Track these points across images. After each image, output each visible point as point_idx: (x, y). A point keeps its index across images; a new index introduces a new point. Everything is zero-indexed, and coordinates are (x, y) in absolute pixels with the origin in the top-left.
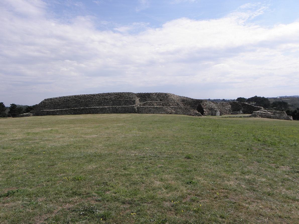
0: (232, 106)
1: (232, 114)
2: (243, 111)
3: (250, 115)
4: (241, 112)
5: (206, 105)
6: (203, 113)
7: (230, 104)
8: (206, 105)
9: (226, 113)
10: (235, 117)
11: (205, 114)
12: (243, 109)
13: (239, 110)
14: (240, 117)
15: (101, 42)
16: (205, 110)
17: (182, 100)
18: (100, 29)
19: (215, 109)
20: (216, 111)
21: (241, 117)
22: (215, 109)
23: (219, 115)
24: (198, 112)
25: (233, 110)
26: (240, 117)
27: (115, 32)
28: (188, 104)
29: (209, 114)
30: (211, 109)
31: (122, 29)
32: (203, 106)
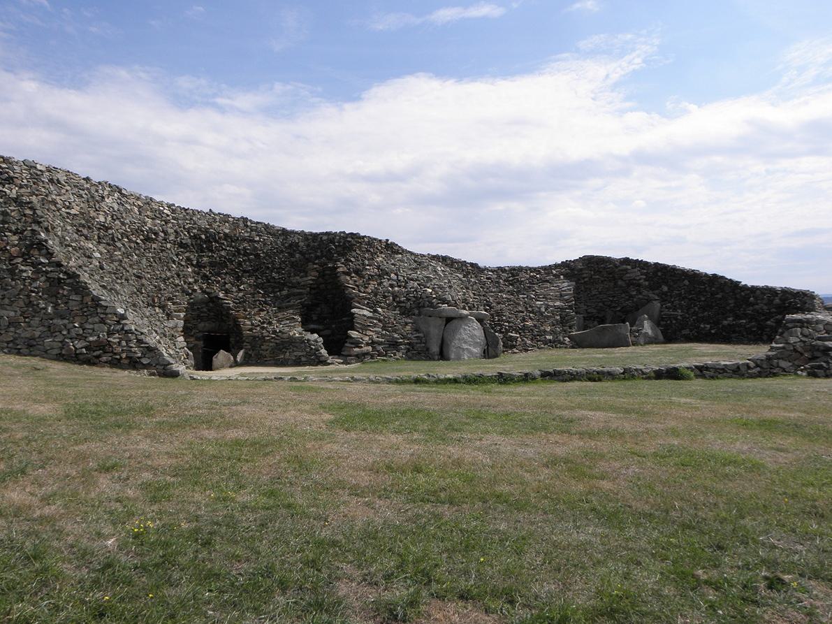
0: (577, 289)
1: (578, 344)
2: (658, 324)
3: (760, 351)
4: (648, 328)
5: (383, 273)
6: (338, 346)
7: (567, 276)
8: (383, 273)
9: (539, 340)
10: (611, 376)
11: (357, 344)
12: (657, 305)
13: (628, 314)
14: (659, 375)
15: (189, 141)
16: (361, 312)
17: (195, 237)
18: (183, 102)
19: (444, 301)
20: (449, 320)
21: (673, 374)
22: (444, 301)
23: (477, 351)
24: (297, 331)
25: (591, 319)
26: (659, 375)
27: (221, 110)
28: (240, 264)
29: (394, 345)
30: (416, 306)
31: (245, 100)
32: (350, 282)
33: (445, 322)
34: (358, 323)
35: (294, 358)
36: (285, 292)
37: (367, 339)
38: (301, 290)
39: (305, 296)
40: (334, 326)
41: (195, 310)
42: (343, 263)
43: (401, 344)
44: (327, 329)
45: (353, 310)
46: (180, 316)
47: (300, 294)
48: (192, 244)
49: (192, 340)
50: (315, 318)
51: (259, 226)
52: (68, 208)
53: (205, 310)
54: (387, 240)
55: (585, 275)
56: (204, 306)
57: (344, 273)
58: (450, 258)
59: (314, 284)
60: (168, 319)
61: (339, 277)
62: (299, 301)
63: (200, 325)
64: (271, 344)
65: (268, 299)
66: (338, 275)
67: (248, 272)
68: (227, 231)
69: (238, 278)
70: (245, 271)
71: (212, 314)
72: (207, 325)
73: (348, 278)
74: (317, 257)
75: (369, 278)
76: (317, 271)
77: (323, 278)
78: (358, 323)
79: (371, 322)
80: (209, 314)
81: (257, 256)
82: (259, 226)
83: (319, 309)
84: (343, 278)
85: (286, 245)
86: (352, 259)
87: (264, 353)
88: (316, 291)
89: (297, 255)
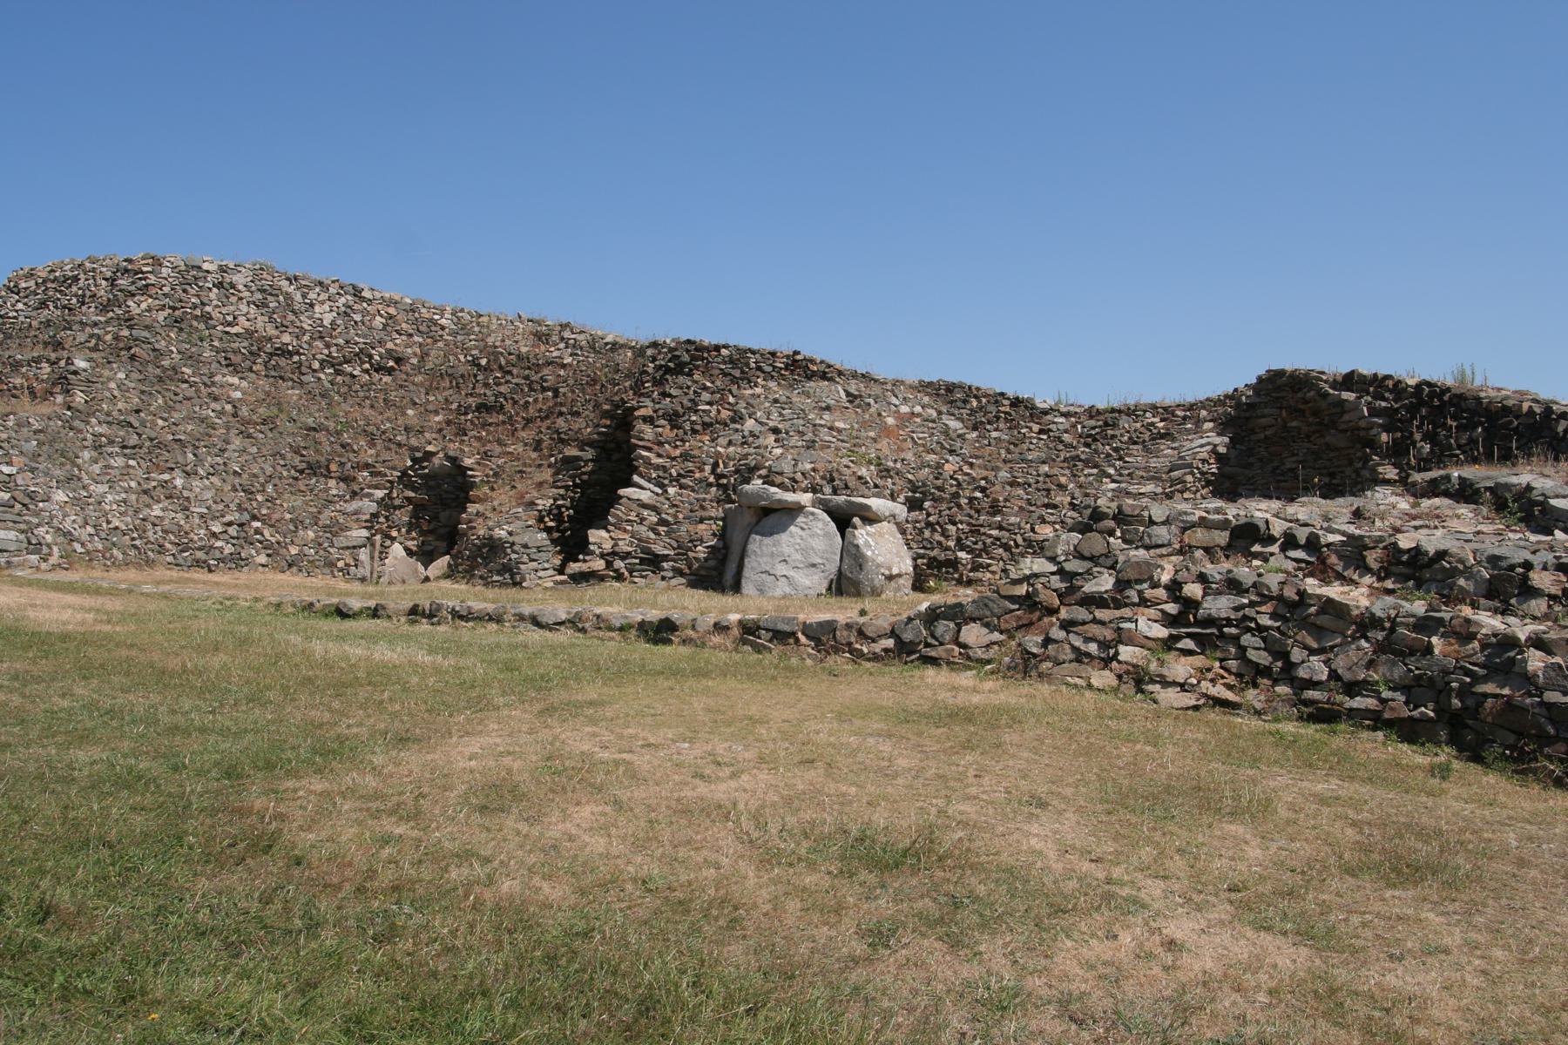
16: (640, 492)
20: (767, 511)
33: (754, 520)
43: (666, 558)
45: (622, 492)
51: (581, 337)
52: (230, 324)
54: (796, 353)
55: (1263, 421)
57: (646, 419)
58: (961, 386)
68: (524, 350)
75: (694, 431)
82: (581, 337)
86: (674, 392)
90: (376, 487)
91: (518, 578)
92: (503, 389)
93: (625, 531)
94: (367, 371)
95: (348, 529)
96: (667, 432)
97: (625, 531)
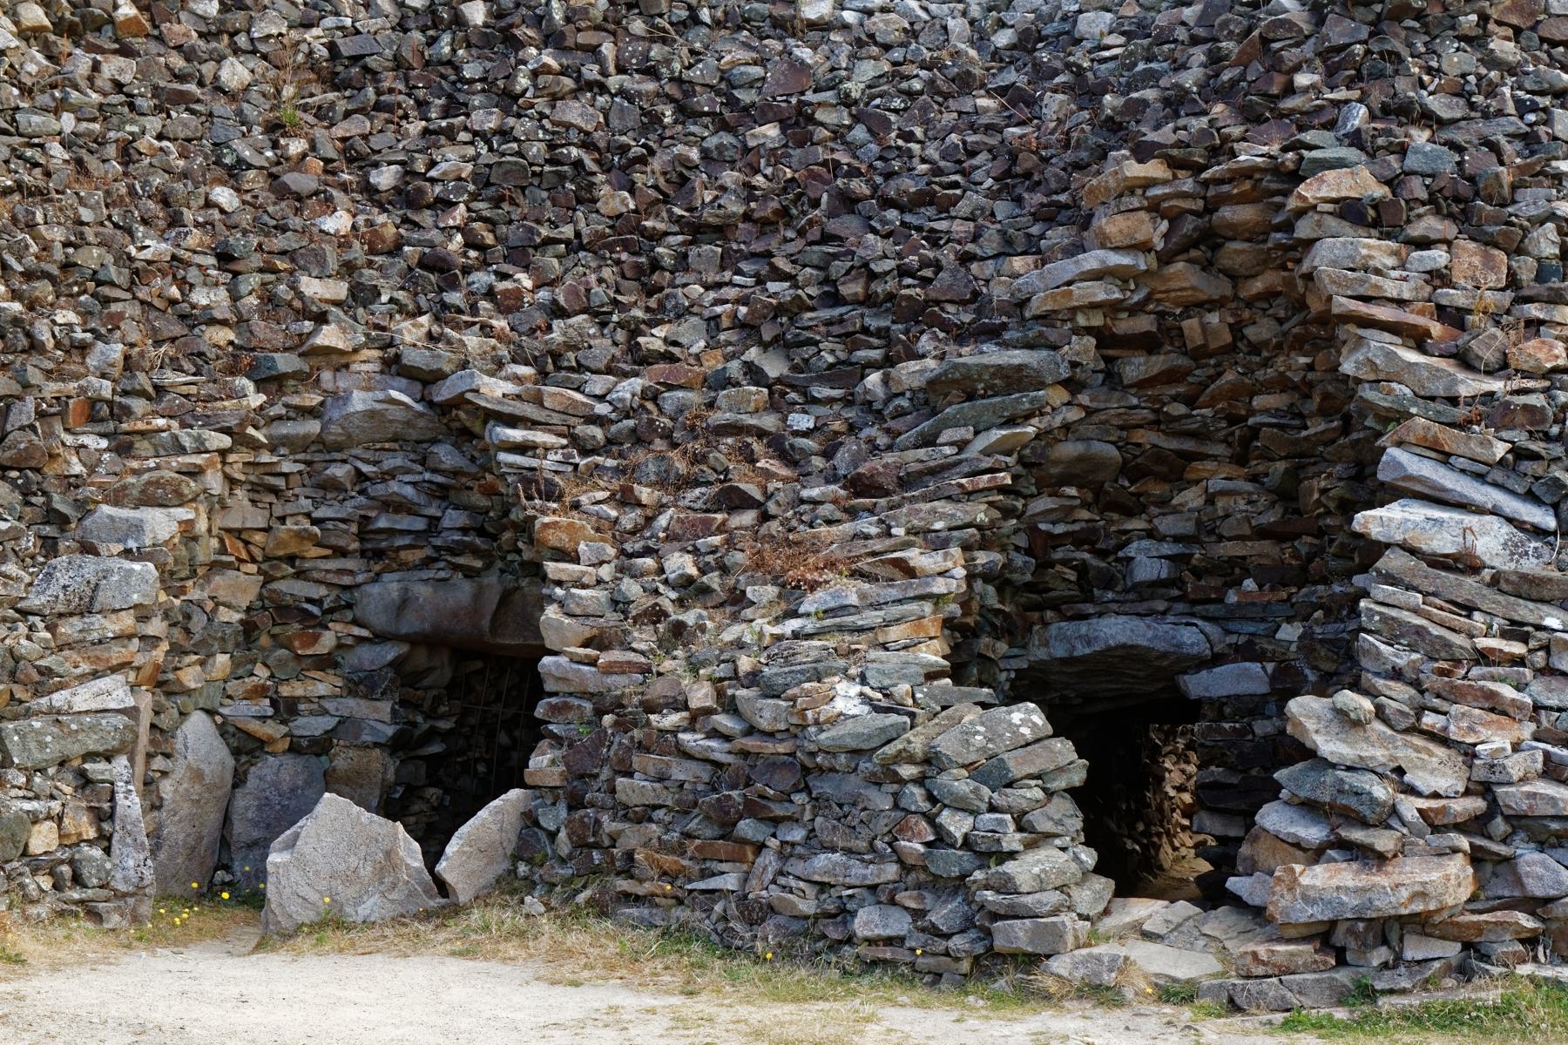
11: (1348, 827)
34: (1395, 633)
35: (807, 906)
36: (910, 373)
37: (1438, 775)
38: (1018, 357)
39: (1058, 396)
40: (1290, 632)
41: (333, 486)
42: (1355, 139)
44: (1248, 652)
45: (1377, 521)
46: (137, 528)
47: (1015, 379)
48: (399, 63)
49: (322, 689)
50: (1147, 563)
53: (401, 488)
56: (397, 461)
57: (1350, 211)
59: (1134, 310)
60: (50, 547)
61: (1309, 243)
62: (997, 434)
63: (375, 589)
64: (681, 771)
65: (802, 421)
66: (1303, 229)
67: (721, 231)
69: (646, 276)
70: (697, 231)
71: (454, 518)
72: (423, 591)
73: (1377, 250)
74: (1176, 103)
76: (1154, 208)
77: (1207, 266)
78: (1395, 633)
79: (1515, 630)
80: (434, 521)
81: (798, 123)
83: (1191, 498)
84: (1338, 253)
85: (1003, 39)
86: (1439, 105)
87: (632, 837)
88: (1158, 363)
89: (1054, 104)
90: (147, 499)
91: (1015, 935)
92: (575, 112)
93: (1496, 706)
94: (28, 35)
95: (46, 681)
96: (1475, 273)
97: (1496, 706)
